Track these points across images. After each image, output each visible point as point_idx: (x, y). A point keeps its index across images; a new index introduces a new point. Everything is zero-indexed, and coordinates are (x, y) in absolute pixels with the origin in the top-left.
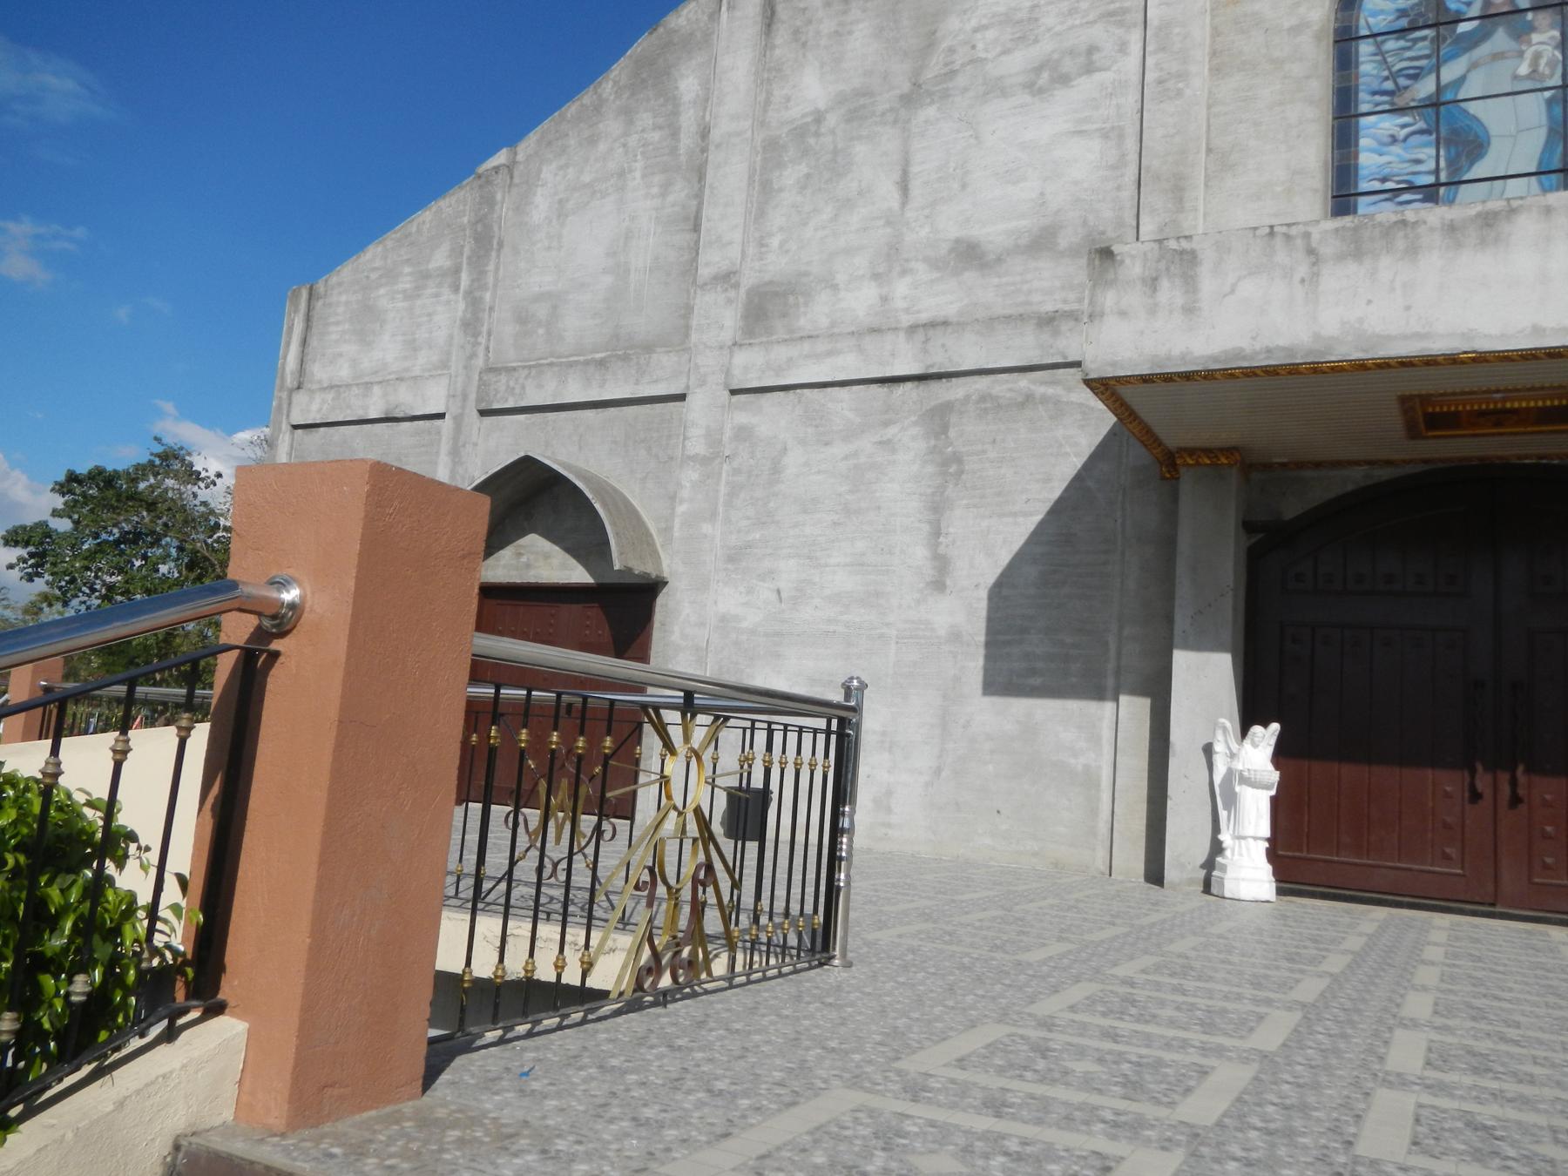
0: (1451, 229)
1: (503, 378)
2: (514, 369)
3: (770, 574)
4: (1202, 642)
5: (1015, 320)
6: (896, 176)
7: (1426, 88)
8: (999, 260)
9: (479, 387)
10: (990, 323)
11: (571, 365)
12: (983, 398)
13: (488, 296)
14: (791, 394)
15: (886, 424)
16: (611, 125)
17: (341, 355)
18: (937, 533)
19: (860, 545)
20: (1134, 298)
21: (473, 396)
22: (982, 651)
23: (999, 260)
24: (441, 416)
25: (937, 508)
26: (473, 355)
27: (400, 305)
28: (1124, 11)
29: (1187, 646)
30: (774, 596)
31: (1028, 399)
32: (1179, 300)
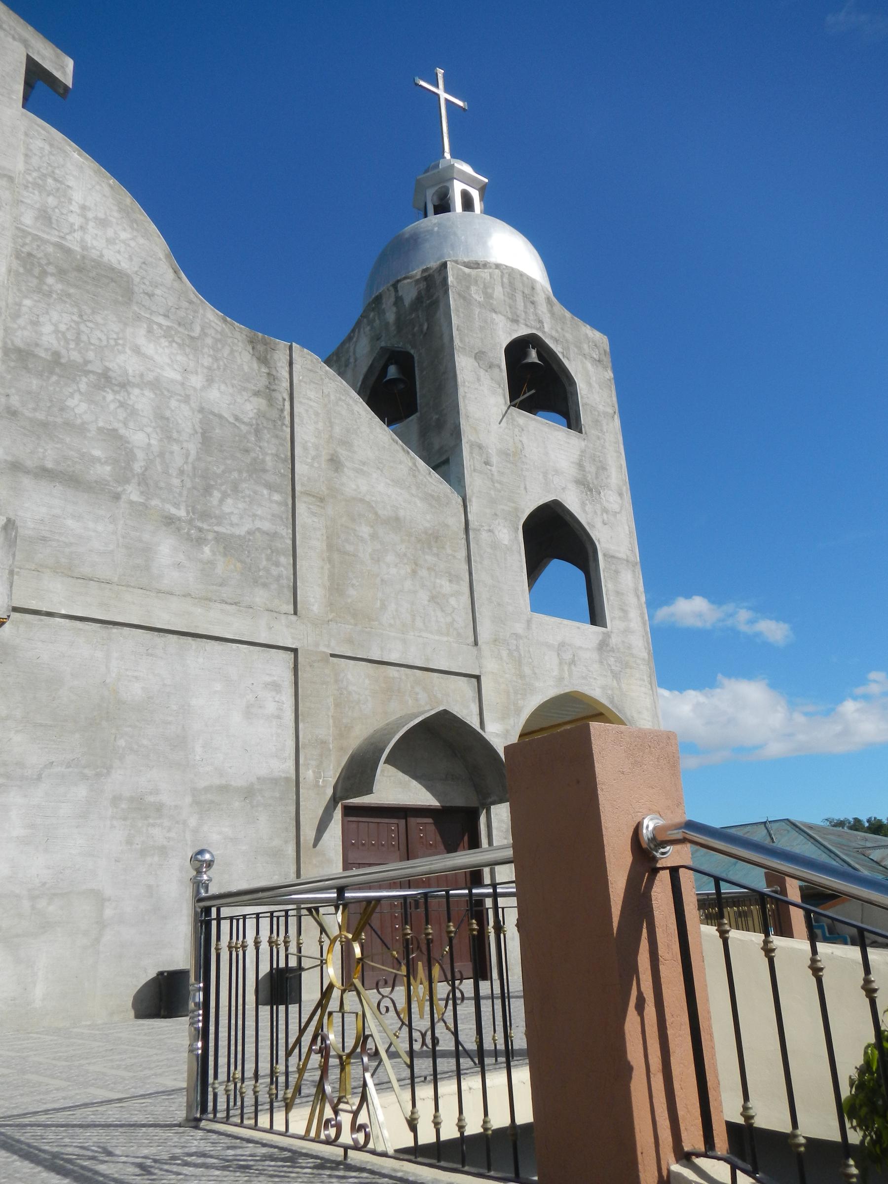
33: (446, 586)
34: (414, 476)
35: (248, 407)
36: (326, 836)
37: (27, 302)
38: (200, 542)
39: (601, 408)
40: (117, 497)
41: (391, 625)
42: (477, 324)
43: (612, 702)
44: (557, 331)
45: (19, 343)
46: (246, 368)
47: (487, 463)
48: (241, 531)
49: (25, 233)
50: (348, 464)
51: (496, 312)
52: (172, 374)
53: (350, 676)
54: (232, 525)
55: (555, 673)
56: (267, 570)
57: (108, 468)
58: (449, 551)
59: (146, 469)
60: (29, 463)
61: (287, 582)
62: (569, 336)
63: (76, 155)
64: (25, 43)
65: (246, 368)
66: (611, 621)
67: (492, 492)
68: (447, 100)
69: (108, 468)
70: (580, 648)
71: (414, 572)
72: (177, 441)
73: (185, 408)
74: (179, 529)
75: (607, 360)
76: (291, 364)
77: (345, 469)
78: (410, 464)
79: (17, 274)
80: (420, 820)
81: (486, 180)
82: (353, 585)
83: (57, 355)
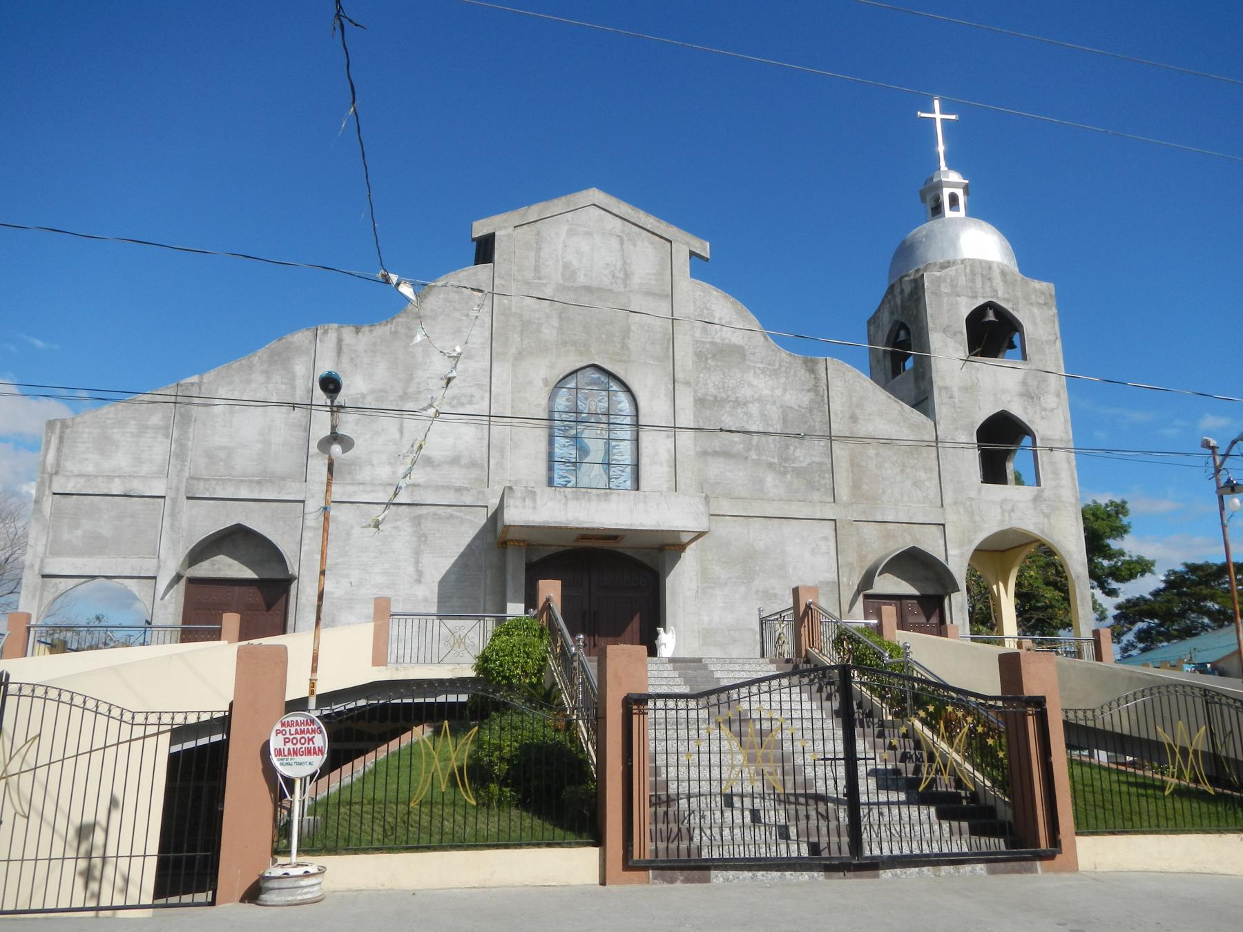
0: (598, 495)
1: (202, 483)
2: (208, 480)
3: (347, 576)
4: (515, 601)
5: (447, 488)
6: (398, 426)
7: (573, 432)
8: (439, 465)
9: (187, 486)
10: (437, 488)
11: (242, 481)
12: (435, 514)
13: (190, 443)
14: (354, 505)
15: (396, 520)
16: (258, 377)
17: (87, 459)
18: (417, 562)
19: (387, 566)
20: (519, 503)
21: (183, 490)
22: (436, 605)
23: (439, 465)
24: (164, 497)
25: (417, 554)
26: (182, 470)
27: (129, 439)
28: (483, 385)
29: (511, 602)
30: (349, 585)
31: (451, 516)
32: (531, 505)
33: (922, 475)
34: (902, 415)
35: (805, 398)
36: (854, 608)
37: (701, 375)
38: (785, 473)
39: (1044, 338)
40: (746, 458)
41: (888, 501)
42: (945, 307)
43: (1042, 531)
44: (1009, 293)
45: (700, 396)
46: (803, 378)
47: (950, 398)
48: (804, 464)
49: (697, 341)
50: (861, 417)
51: (959, 296)
52: (766, 392)
53: (865, 530)
54: (800, 462)
55: (999, 518)
56: (819, 482)
57: (741, 446)
58: (925, 455)
59: (758, 442)
60: (709, 450)
61: (829, 486)
62: (1019, 294)
63: (715, 292)
64: (688, 244)
65: (803, 378)
66: (1045, 480)
67: (955, 415)
68: (942, 119)
69: (741, 446)
70: (1019, 501)
71: (902, 471)
72: (771, 425)
73: (774, 407)
74: (775, 469)
75: (1053, 302)
76: (827, 369)
77: (860, 421)
78: (899, 409)
79: (696, 362)
80: (908, 601)
81: (967, 182)
82: (866, 483)
83: (716, 397)
